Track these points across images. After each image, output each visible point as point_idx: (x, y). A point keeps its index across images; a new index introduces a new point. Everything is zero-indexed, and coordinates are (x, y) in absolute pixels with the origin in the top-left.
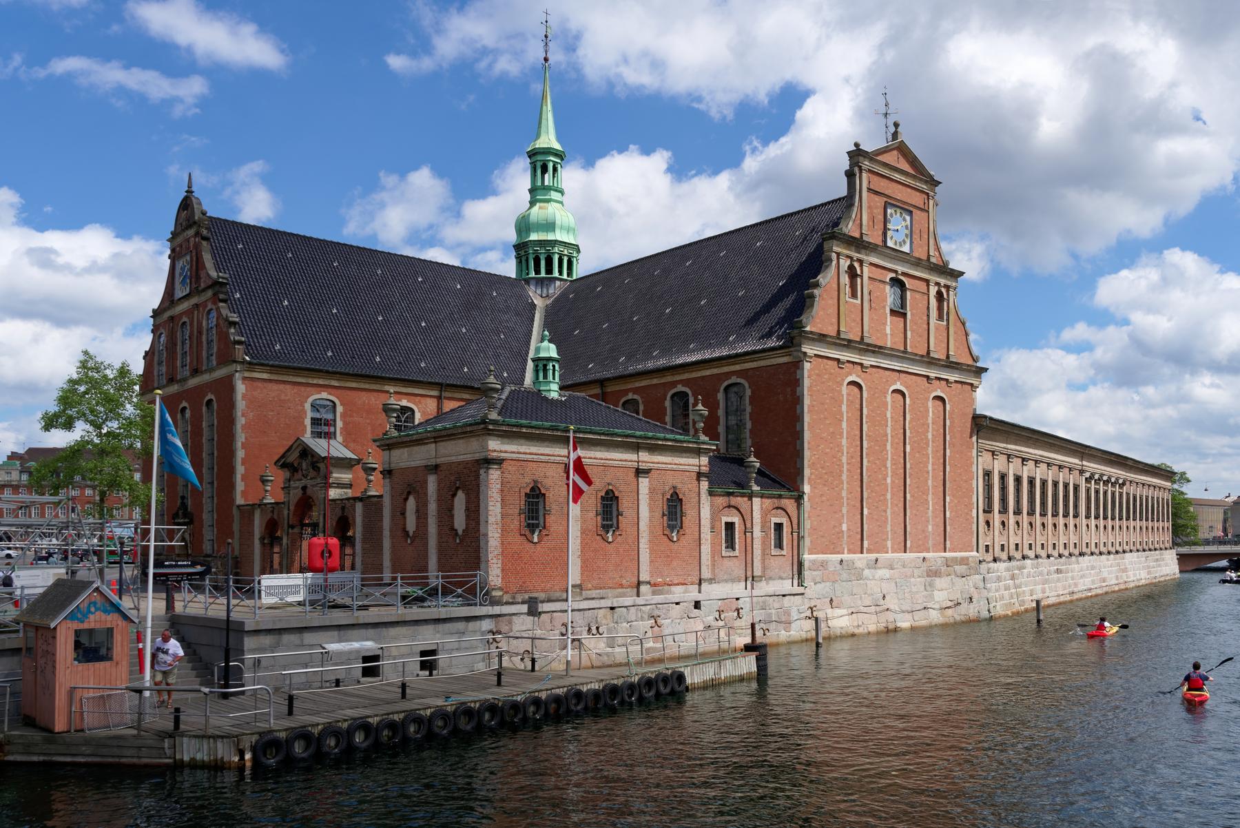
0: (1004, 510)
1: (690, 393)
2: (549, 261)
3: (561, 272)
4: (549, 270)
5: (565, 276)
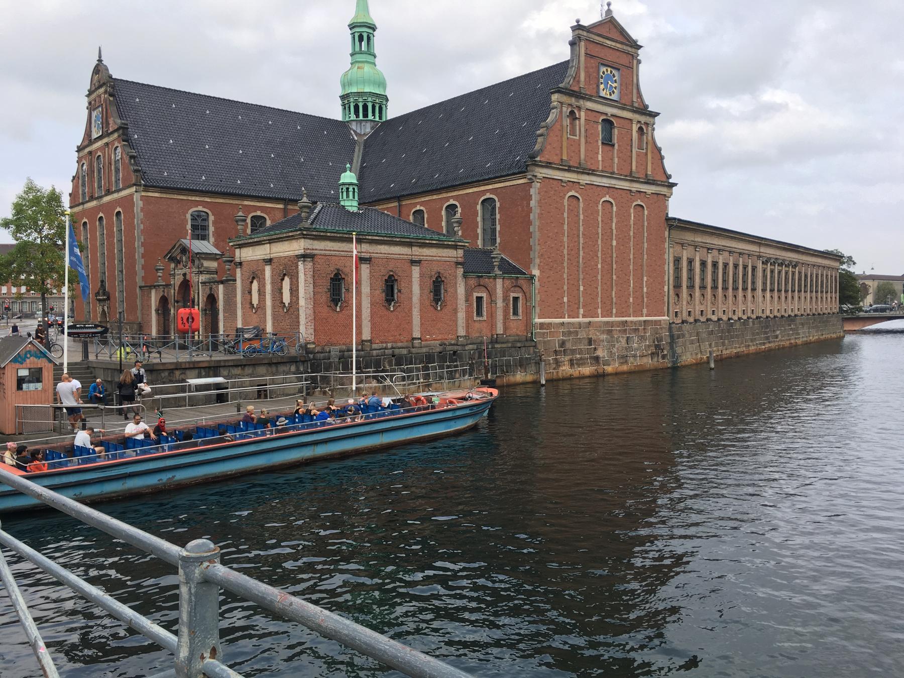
0: (745, 289)
1: (497, 199)
2: (365, 107)
3: (374, 115)
4: (366, 115)
5: (377, 119)
